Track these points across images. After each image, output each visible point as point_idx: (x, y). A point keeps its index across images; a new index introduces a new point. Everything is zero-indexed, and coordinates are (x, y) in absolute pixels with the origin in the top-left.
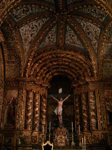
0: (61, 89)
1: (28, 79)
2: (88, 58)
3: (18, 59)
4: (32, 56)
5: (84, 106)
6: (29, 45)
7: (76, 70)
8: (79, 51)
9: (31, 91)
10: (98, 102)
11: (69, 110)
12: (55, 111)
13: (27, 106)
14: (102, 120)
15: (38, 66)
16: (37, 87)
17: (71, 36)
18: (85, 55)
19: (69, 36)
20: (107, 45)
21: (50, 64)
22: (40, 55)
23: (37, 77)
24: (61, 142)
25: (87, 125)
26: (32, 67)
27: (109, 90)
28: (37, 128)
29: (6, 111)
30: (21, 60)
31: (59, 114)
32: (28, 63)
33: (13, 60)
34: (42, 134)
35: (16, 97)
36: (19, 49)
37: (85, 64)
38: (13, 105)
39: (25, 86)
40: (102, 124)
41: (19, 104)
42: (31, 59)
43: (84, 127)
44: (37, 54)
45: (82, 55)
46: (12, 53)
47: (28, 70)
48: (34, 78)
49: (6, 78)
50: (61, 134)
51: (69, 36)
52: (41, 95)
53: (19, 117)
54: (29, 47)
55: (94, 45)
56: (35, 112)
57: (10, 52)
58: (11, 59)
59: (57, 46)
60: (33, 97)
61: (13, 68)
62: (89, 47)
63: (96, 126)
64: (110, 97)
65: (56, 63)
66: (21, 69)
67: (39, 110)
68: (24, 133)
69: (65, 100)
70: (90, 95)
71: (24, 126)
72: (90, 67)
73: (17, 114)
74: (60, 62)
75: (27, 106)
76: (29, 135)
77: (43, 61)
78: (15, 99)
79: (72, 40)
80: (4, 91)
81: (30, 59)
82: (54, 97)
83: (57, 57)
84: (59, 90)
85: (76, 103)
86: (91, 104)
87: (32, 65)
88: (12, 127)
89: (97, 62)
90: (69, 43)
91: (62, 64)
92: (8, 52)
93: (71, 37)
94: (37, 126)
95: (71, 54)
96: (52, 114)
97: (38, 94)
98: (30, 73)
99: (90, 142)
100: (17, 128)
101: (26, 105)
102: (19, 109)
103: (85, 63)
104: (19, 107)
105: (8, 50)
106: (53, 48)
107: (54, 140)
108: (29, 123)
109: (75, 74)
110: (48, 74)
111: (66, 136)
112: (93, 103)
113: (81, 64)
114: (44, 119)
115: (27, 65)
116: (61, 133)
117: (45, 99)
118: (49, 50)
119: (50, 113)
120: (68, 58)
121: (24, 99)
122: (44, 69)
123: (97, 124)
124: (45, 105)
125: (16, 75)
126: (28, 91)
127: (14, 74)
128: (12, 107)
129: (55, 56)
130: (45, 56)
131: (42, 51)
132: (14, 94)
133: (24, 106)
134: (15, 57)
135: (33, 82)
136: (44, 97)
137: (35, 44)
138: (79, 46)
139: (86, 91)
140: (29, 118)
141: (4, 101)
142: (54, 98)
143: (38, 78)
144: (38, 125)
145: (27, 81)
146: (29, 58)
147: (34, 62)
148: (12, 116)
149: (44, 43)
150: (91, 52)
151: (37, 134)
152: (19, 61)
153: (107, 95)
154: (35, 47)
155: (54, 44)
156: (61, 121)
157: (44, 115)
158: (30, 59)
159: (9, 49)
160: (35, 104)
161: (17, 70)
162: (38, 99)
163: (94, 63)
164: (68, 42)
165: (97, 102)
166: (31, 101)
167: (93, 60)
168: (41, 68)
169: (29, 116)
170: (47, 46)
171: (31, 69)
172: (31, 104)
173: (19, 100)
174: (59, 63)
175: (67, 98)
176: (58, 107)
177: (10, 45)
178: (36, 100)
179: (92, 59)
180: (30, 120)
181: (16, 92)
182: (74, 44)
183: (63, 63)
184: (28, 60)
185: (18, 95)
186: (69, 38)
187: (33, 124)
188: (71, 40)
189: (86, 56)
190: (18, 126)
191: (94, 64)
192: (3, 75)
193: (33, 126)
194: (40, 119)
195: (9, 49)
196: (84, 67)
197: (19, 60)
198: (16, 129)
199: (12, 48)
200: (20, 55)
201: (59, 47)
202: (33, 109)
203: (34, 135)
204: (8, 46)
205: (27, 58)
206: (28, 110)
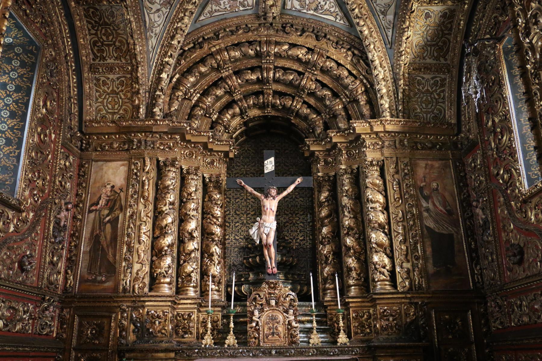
1: (164, 125)
2: (361, 57)
3: (128, 57)
4: (175, 48)
5: (346, 213)
6: (164, 9)
7: (321, 99)
8: (331, 34)
9: (173, 165)
10: (395, 200)
11: (297, 231)
12: (251, 232)
13: (158, 215)
14: (409, 257)
15: (194, 85)
16: (191, 154)
18: (352, 49)
20: (426, 11)
21: (235, 81)
22: (201, 48)
23: (193, 120)
24: (273, 334)
25: (359, 275)
26: (175, 88)
27: (429, 162)
28: (194, 287)
29: (86, 233)
30: (136, 59)
31: (267, 240)
32: (160, 72)
33: (109, 61)
35: (122, 185)
36: (130, 22)
37: (350, 77)
38: (111, 210)
39: (153, 148)
40: (408, 272)
41: (131, 206)
42: (172, 61)
43: (348, 282)
44: (192, 45)
45: (342, 47)
46: (104, 38)
47: (163, 97)
48: (180, 123)
49: (86, 122)
50: (272, 306)
52: (204, 178)
53: (130, 249)
54: (163, 18)
55: (383, 13)
56: (187, 235)
57: (99, 32)
58: (104, 59)
59: (258, 17)
60: (178, 184)
61: (111, 89)
62: (364, 21)
63: (388, 278)
64: (435, 184)
65: (254, 77)
66: (138, 92)
67: (199, 229)
68: (147, 303)
69: (285, 193)
70: (367, 177)
71: (147, 280)
72: (369, 86)
73: (122, 243)
74: (268, 73)
75: (158, 215)
76: (164, 312)
77: (212, 69)
78: (119, 192)
80: (81, 166)
81: (167, 59)
82: (247, 186)
83: (258, 55)
84: (266, 162)
85: (321, 204)
86: (371, 205)
87: (174, 80)
88: (107, 284)
89: (390, 71)
90: (298, 7)
91: (276, 81)
92: (93, 32)
94: (193, 279)
95: (304, 46)
96: (242, 243)
97: (196, 174)
98: (170, 105)
99: (369, 333)
100: (124, 288)
101: (154, 212)
102: (132, 225)
103: (350, 73)
104: (131, 216)
105: (90, 26)
106: (246, 25)
107: (249, 325)
108: (166, 271)
109: (319, 113)
110: (230, 113)
111: (291, 311)
112: (377, 205)
113: (338, 79)
114: (216, 258)
115: (159, 80)
116: (273, 302)
117: (220, 193)
119: (235, 239)
120: (298, 60)
121: (150, 191)
122: (217, 96)
123: (393, 273)
124: (218, 212)
125: (121, 112)
126: (162, 164)
127: (113, 108)
128: (107, 219)
129: (250, 51)
130: (219, 52)
132: (114, 174)
133: (149, 215)
134: (118, 49)
135: (178, 137)
136: (215, 187)
137: (186, 10)
138: (332, 18)
139: (355, 167)
140: (163, 253)
141: (81, 196)
142: (250, 189)
143: (196, 124)
144: (195, 277)
145: (156, 133)
146: (165, 55)
147: (182, 72)
148: (105, 246)
149: (214, 8)
150: (371, 36)
151: (192, 306)
152: (131, 63)
153: (424, 177)
154: (186, 20)
155: (250, 12)
156: (274, 265)
157: (217, 245)
158: (167, 59)
159: (93, 22)
160: (186, 209)
161: (123, 97)
162: (196, 191)
163: (380, 72)
165: (393, 200)
166: (171, 197)
167: (377, 62)
168: (205, 93)
169: (166, 248)
170: (226, 19)
172: (171, 207)
173: (130, 193)
174: (265, 75)
175: (292, 187)
176: (263, 217)
177: (98, 7)
178: (190, 194)
179: (376, 58)
180: (168, 261)
181: (122, 168)
182: (316, 10)
184: (162, 61)
185: (128, 178)
187: (178, 275)
189: (353, 53)
190: (126, 280)
191: (381, 77)
192: (75, 110)
193: (180, 280)
194: (202, 257)
195: (95, 22)
196: (346, 87)
197: (129, 62)
198: (121, 291)
199: (106, 20)
200: (134, 44)
201: (264, 21)
202: (180, 225)
203: (181, 312)
204: (91, 10)
205: (159, 55)
206: (162, 228)
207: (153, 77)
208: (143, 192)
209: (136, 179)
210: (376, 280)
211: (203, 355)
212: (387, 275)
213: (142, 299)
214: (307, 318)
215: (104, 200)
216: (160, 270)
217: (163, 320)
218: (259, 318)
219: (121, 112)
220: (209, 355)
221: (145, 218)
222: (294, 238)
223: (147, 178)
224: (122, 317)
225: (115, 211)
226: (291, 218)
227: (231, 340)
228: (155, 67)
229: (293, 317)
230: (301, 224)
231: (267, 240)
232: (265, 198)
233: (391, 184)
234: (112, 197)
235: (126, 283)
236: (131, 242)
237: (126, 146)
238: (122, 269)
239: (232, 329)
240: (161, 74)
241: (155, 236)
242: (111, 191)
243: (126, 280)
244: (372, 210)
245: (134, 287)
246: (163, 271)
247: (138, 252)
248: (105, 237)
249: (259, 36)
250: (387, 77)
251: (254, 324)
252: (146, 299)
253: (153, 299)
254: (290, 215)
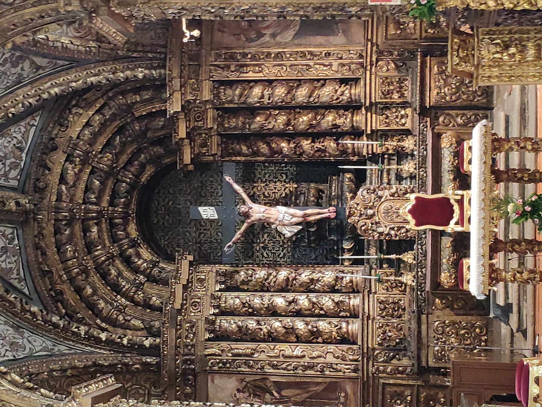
10: (260, 72)
31: (299, 217)
32: (98, 341)
34: (373, 281)
35: (237, 380)
39: (193, 346)
41: (262, 368)
50: (374, 213)
53: (311, 367)
63: (348, 87)
68: (370, 346)
69: (244, 196)
71: (345, 347)
76: (380, 327)
81: (83, 333)
88: (349, 391)
102: (284, 366)
104: (274, 367)
107: (393, 238)
111: (380, 193)
112: (266, 93)
116: (370, 212)
118: (44, 254)
125: (148, 386)
128: (276, 394)
131: (45, 283)
133: (272, 347)
140: (315, 329)
155: (20, 232)
169: (310, 327)
171: (122, 328)
180: (323, 325)
185: (230, 374)
190: (345, 369)
191: (111, 76)
198: (356, 375)
207: (104, 349)
208: (246, 355)
209: (230, 363)
210: (349, 100)
211: (423, 285)
212: (345, 88)
213: (365, 351)
214: (385, 175)
215: (254, 400)
216: (334, 333)
217: (387, 328)
218: (386, 226)
219: (148, 386)
220: (423, 280)
221: (276, 351)
222: (284, 185)
223: (229, 351)
224: (384, 372)
225: (267, 386)
227: (408, 257)
228: (91, 347)
229: (386, 191)
230: (267, 176)
231: (299, 217)
233: (242, 75)
234: (251, 391)
235: (347, 369)
236: (302, 366)
237: (190, 377)
238: (332, 374)
239: (398, 256)
240: (101, 339)
241: (295, 340)
242: (244, 392)
243: (345, 369)
244: (271, 99)
245: (351, 361)
246: (335, 329)
247: (313, 358)
248: (298, 395)
249: (49, 220)
250: (111, 69)
251: (393, 232)
252: (365, 346)
253: (365, 339)
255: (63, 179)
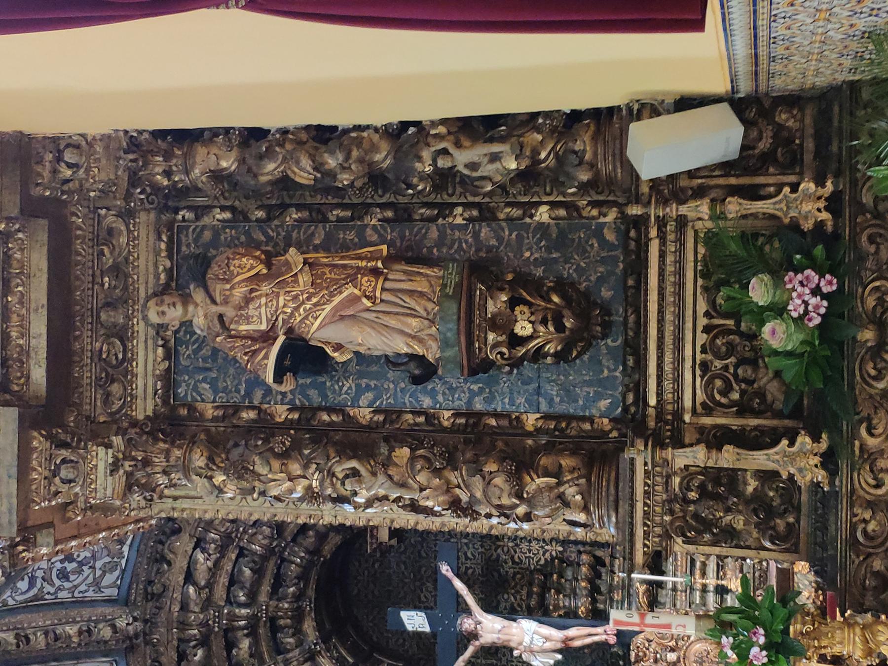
0: (404, 615)
17: (71, 566)
19: (68, 580)
51: (72, 578)
79: (101, 559)
84: (410, 628)
90: (117, 573)
93: (74, 565)
164: (109, 579)
176: (513, 645)
182: (121, 542)
183: (243, 598)
186: (81, 578)
188: (99, 564)
222: (542, 547)
226: (506, 549)
232: (478, 639)
254: (499, 551)
255: (189, 577)
